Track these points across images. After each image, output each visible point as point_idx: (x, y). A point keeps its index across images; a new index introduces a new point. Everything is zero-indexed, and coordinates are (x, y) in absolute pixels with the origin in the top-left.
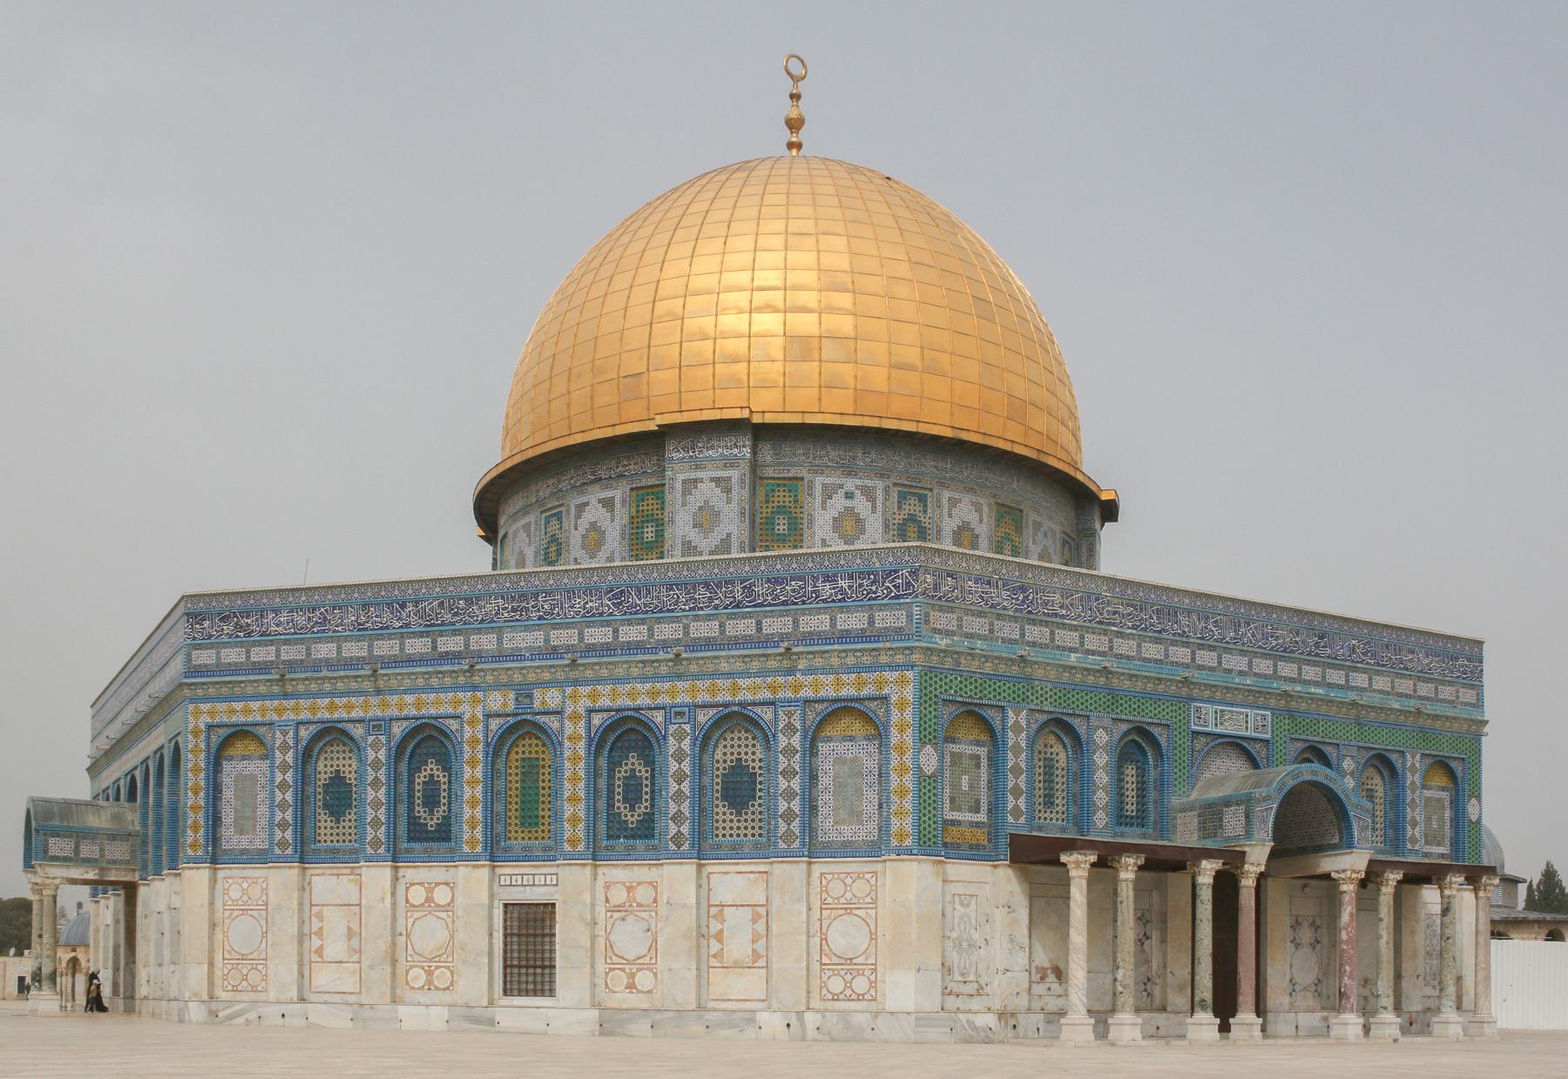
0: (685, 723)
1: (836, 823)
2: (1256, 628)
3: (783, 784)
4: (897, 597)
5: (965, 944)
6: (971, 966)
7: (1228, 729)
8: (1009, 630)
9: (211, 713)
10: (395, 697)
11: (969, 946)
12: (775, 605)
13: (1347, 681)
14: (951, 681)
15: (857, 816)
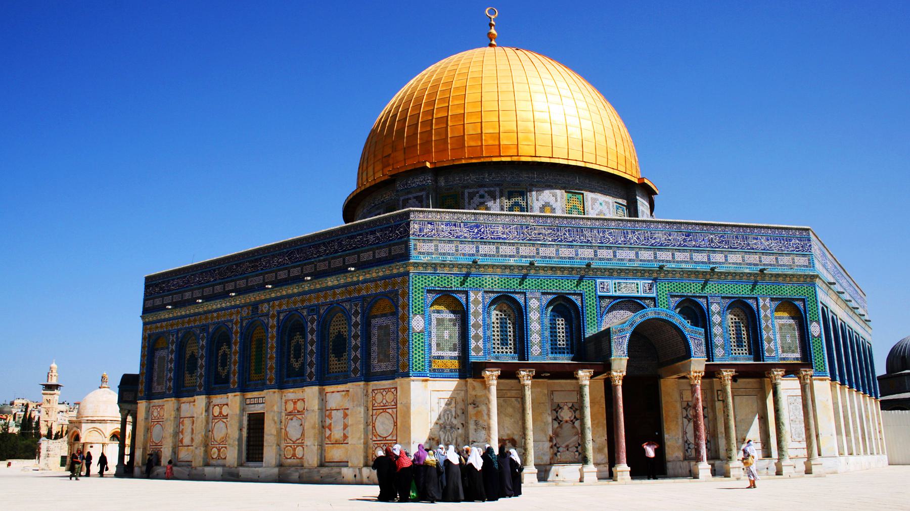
0: (314, 315)
1: (378, 362)
2: (639, 234)
3: (353, 343)
4: (401, 238)
5: (448, 427)
6: (452, 440)
7: (624, 292)
8: (469, 249)
9: (150, 329)
10: (210, 315)
11: (451, 428)
12: (350, 250)
13: (709, 259)
14: (432, 279)
15: (387, 358)
